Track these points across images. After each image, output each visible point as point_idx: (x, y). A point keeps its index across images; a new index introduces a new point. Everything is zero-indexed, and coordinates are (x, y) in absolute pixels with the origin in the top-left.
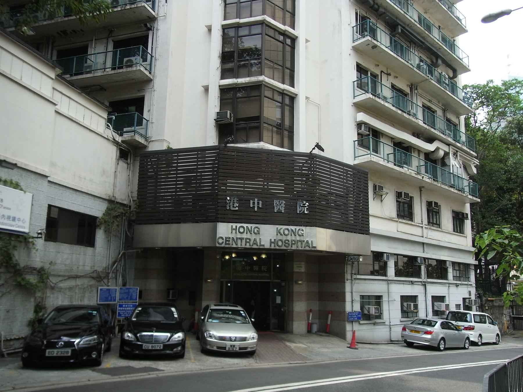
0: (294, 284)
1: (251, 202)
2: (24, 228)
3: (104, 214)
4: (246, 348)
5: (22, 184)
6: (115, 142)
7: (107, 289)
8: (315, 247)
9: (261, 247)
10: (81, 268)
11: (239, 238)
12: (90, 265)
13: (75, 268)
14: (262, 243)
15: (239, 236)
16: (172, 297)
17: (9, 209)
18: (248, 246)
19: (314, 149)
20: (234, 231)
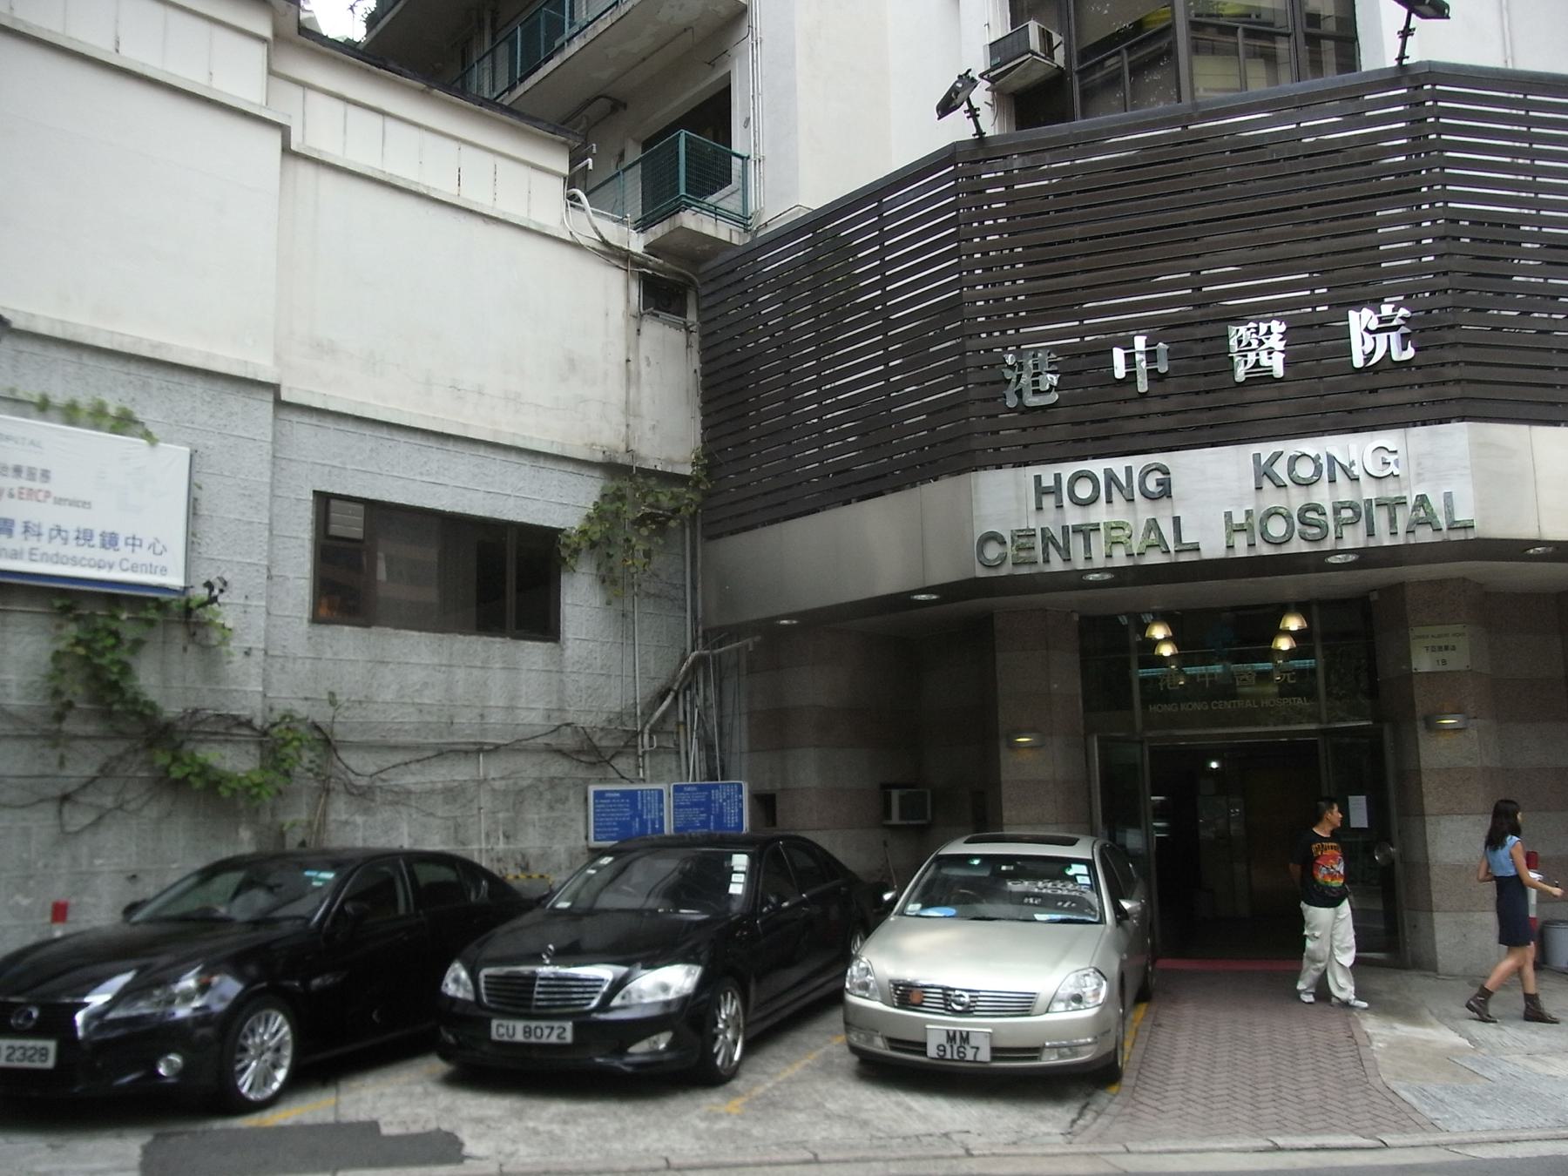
0: (1421, 732)
1: (1119, 355)
2: (164, 571)
3: (589, 518)
4: (1034, 1051)
5: (147, 414)
6: (613, 254)
7: (624, 794)
8: (1468, 527)
9: (1184, 558)
10: (495, 718)
11: (1077, 530)
12: (540, 705)
13: (465, 718)
14: (1187, 538)
15: (1074, 517)
16: (902, 818)
17: (86, 504)
18: (1120, 559)
19: (1406, 33)
20: (1048, 502)
